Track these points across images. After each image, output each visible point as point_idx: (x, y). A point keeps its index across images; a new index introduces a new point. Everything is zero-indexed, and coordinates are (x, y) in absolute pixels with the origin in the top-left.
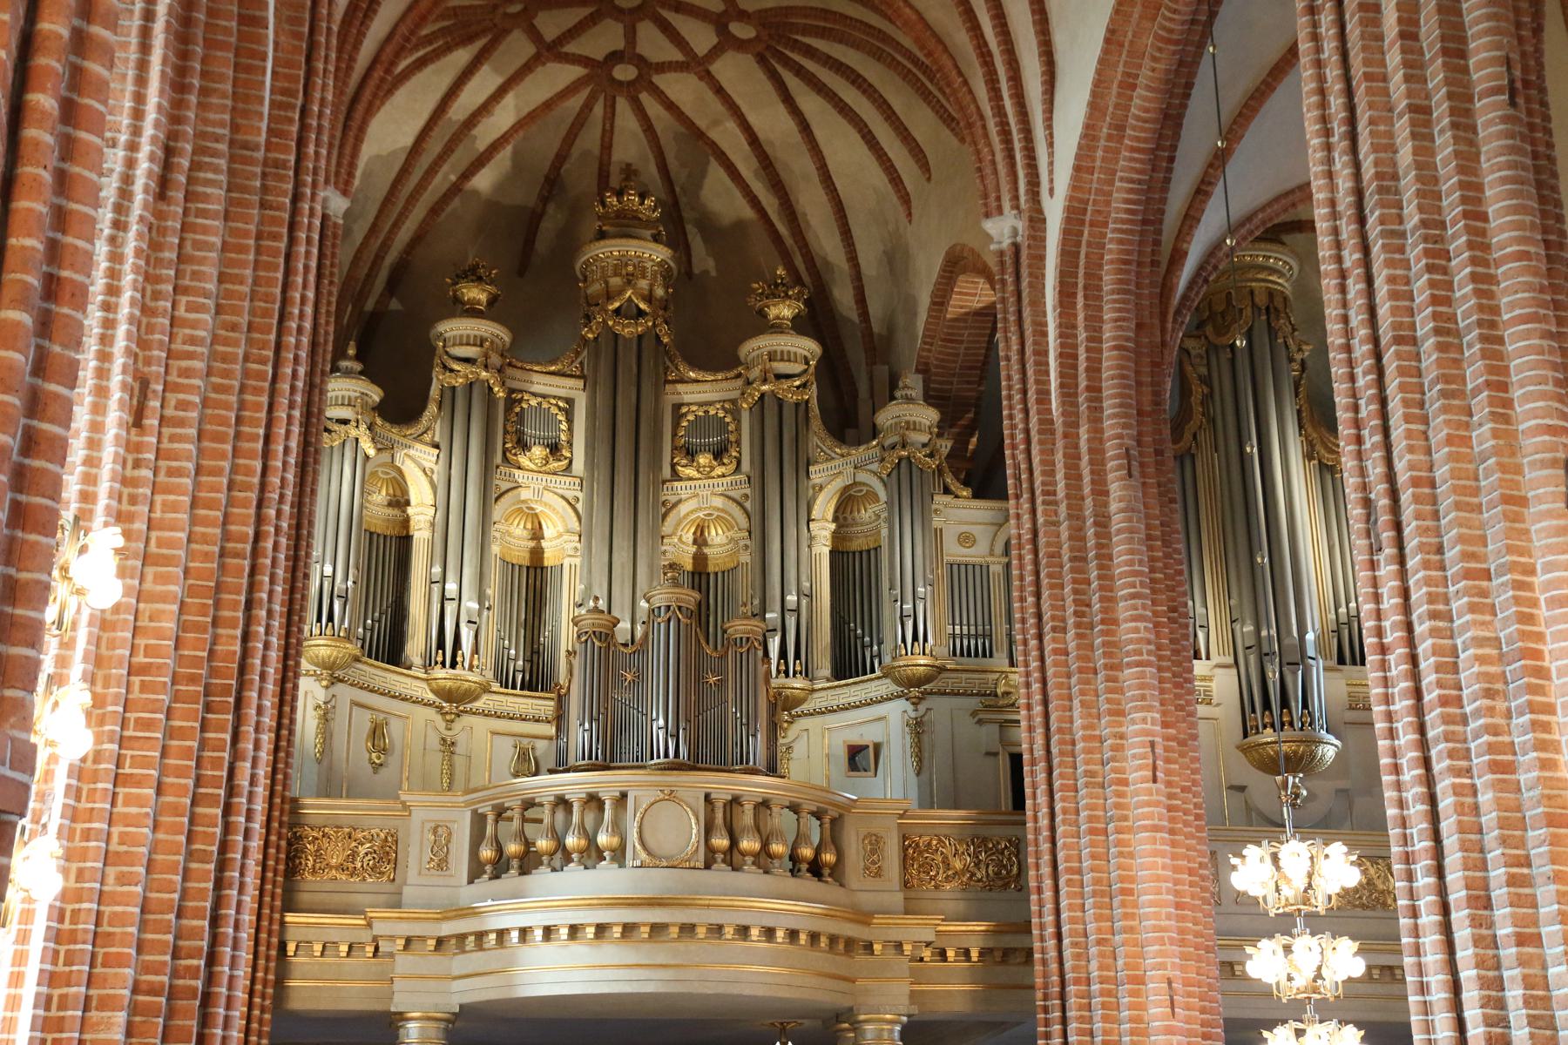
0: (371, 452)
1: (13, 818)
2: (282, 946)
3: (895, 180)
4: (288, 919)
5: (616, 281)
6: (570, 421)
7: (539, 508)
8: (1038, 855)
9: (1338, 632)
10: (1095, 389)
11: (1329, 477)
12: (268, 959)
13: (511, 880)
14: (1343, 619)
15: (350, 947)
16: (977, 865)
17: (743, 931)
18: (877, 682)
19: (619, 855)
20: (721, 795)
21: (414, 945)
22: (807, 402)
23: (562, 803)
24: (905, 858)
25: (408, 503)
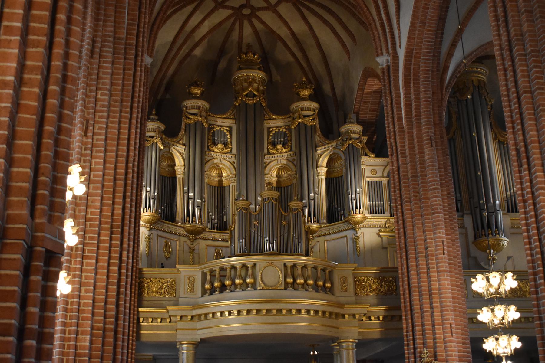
0: (162, 148)
1: (60, 255)
3: (344, 45)
4: (140, 310)
5: (245, 85)
6: (231, 135)
7: (221, 166)
8: (403, 282)
9: (507, 201)
10: (418, 116)
11: (502, 146)
12: (133, 323)
13: (217, 295)
14: (509, 196)
15: (161, 320)
16: (381, 286)
17: (299, 311)
18: (343, 224)
19: (254, 286)
20: (289, 265)
21: (183, 318)
22: (315, 125)
23: (233, 267)
24: (355, 286)
25: (175, 165)
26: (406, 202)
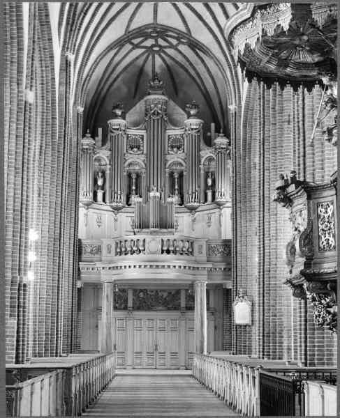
2: (79, 268)
5: (152, 106)
13: (123, 256)
20: (165, 239)
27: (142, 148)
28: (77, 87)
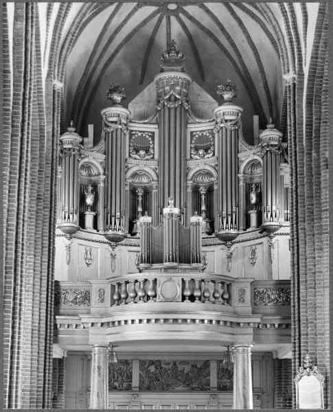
2: (55, 325)
5: (167, 88)
20: (187, 280)
26: (301, 221)
27: (152, 151)
28: (52, 49)
